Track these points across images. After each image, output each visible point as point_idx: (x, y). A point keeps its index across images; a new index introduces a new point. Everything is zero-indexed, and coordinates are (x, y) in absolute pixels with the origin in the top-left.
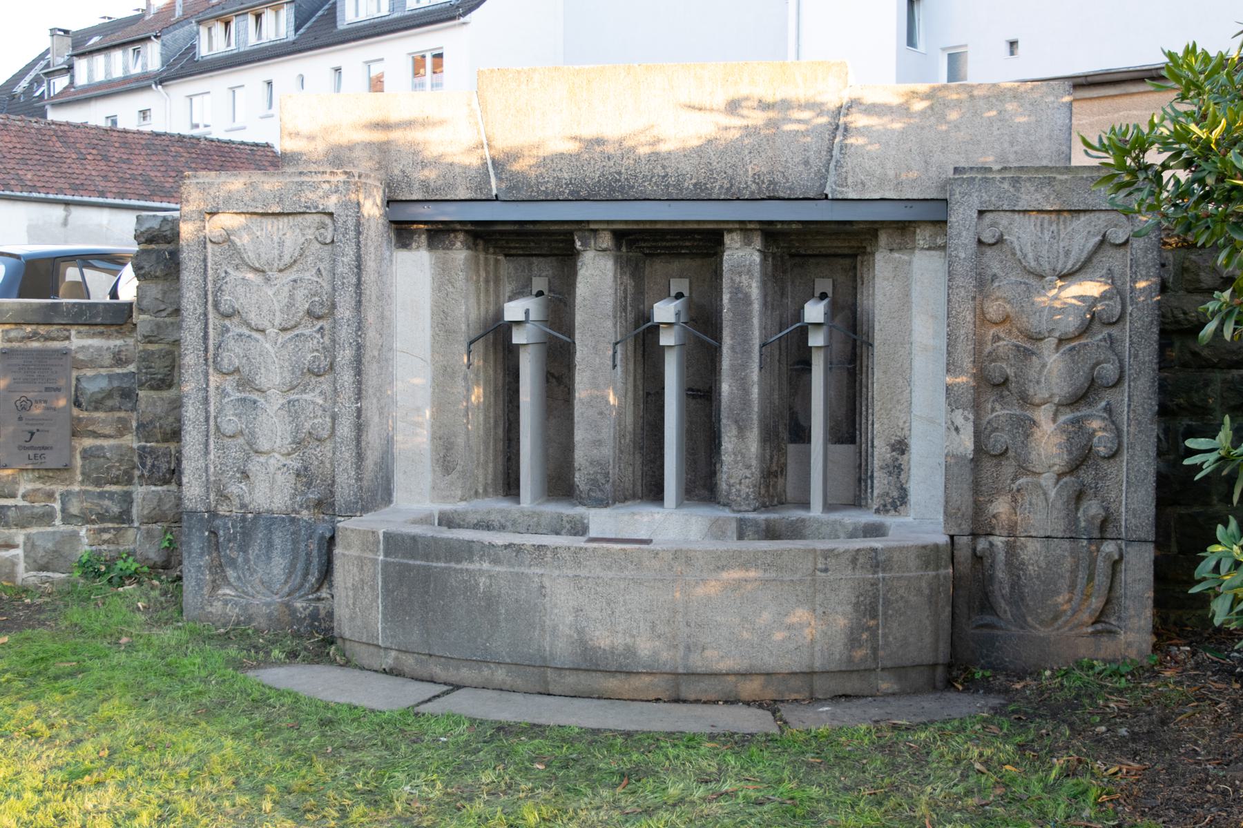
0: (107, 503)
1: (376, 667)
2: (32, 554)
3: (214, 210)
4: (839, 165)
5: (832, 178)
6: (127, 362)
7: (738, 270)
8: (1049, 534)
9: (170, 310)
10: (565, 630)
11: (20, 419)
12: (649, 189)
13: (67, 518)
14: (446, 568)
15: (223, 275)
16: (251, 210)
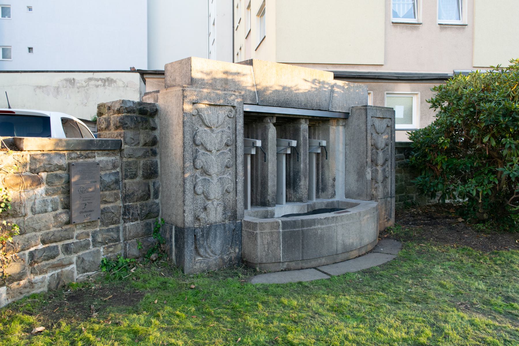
0: (112, 233)
1: (278, 270)
2: (82, 265)
3: (196, 102)
4: (332, 102)
5: (330, 105)
6: (117, 167)
7: (304, 131)
9: (136, 143)
10: (340, 242)
12: (295, 105)
14: (308, 229)
15: (197, 128)
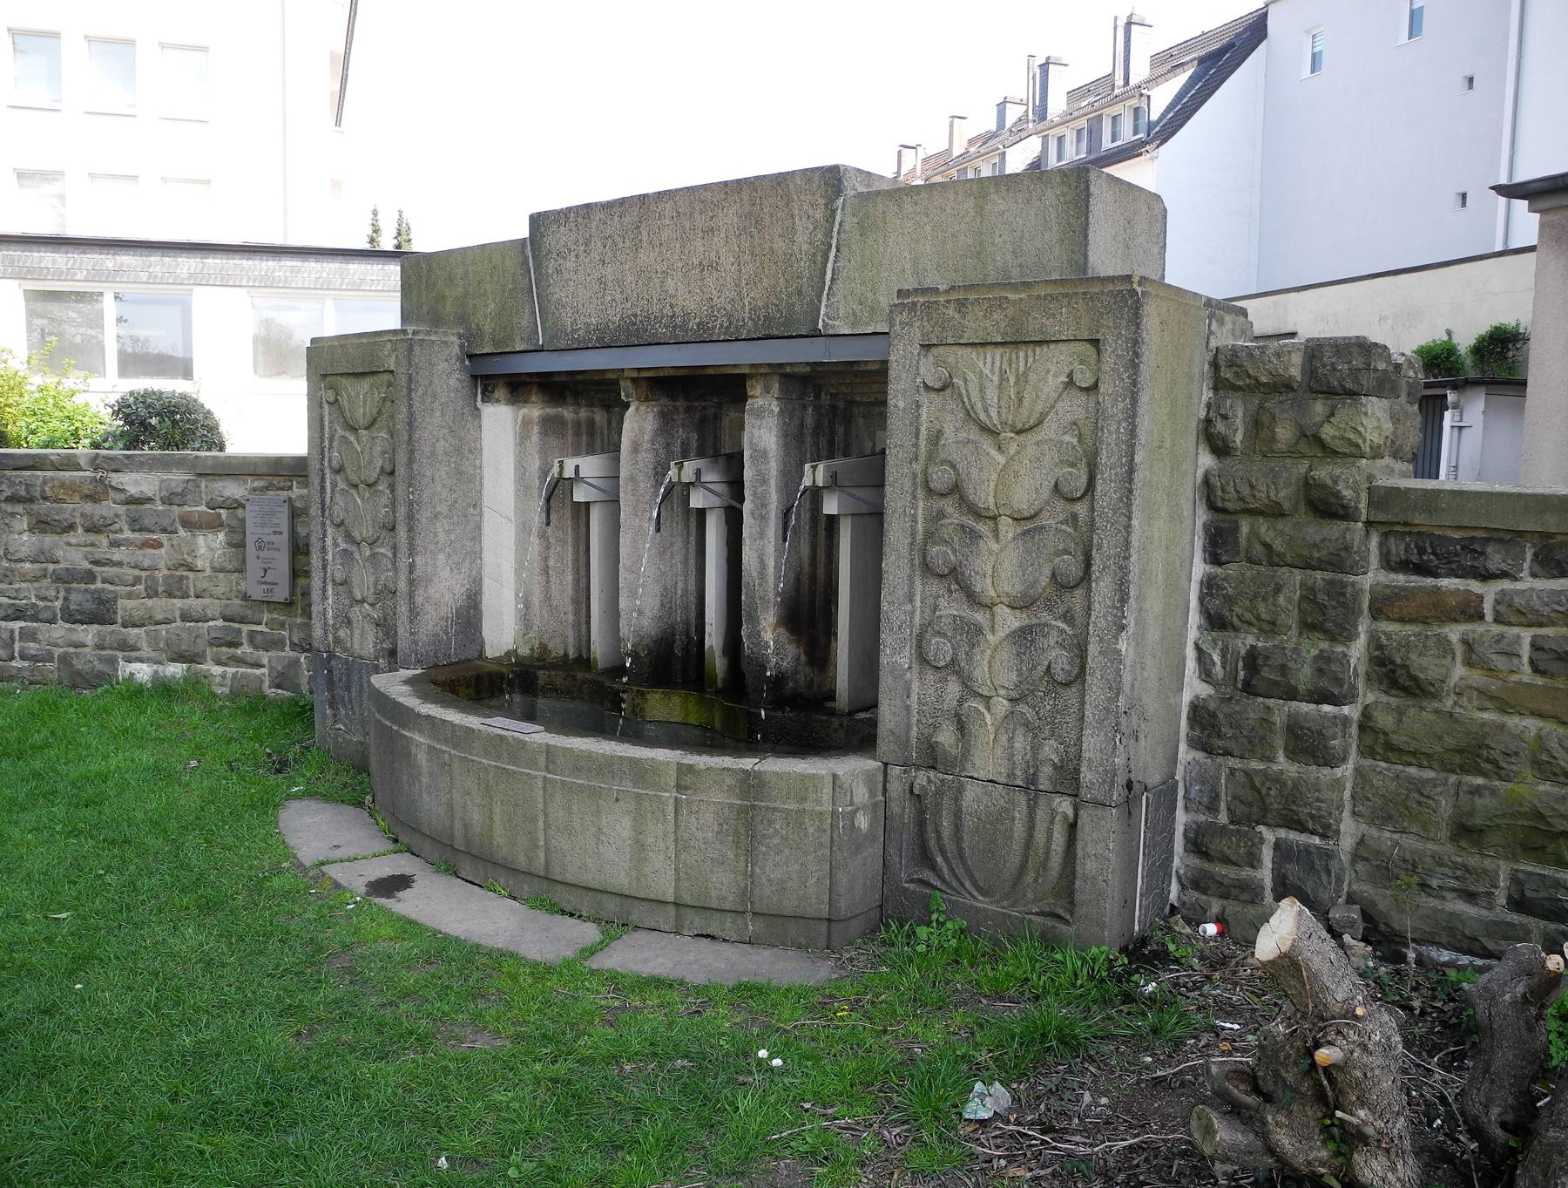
8: (991, 778)
11: (258, 557)
13: (293, 646)
16: (346, 371)
